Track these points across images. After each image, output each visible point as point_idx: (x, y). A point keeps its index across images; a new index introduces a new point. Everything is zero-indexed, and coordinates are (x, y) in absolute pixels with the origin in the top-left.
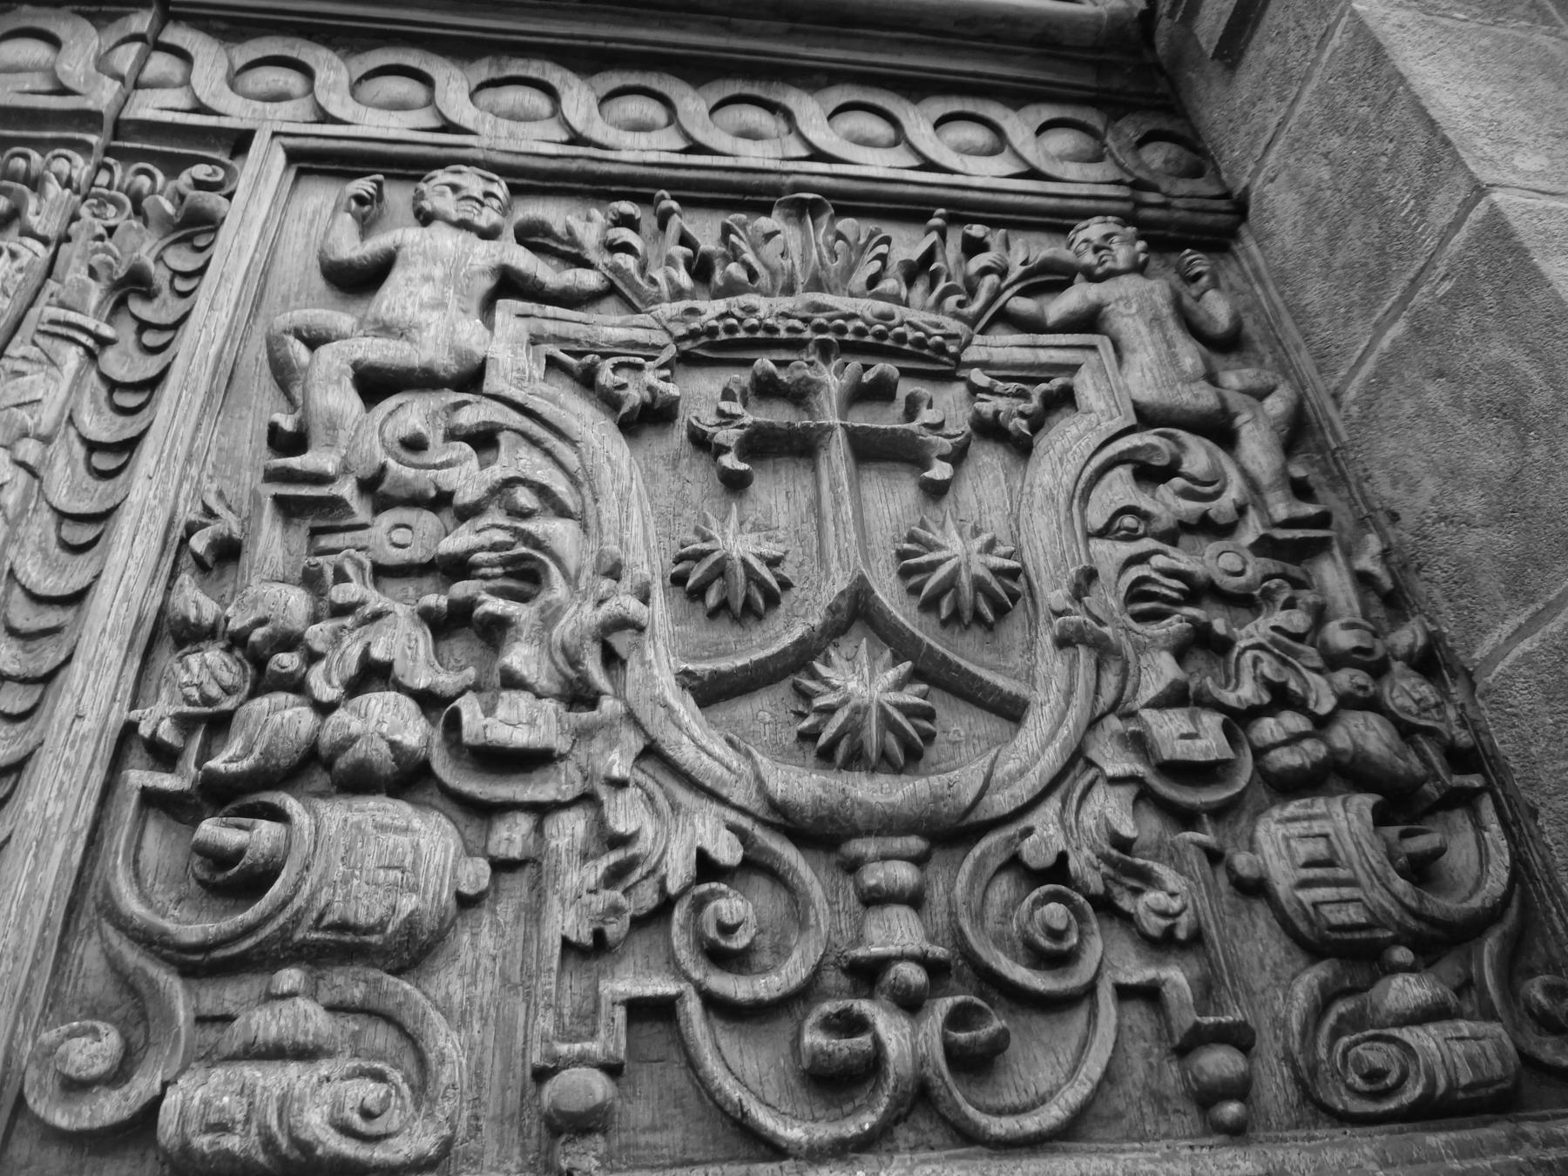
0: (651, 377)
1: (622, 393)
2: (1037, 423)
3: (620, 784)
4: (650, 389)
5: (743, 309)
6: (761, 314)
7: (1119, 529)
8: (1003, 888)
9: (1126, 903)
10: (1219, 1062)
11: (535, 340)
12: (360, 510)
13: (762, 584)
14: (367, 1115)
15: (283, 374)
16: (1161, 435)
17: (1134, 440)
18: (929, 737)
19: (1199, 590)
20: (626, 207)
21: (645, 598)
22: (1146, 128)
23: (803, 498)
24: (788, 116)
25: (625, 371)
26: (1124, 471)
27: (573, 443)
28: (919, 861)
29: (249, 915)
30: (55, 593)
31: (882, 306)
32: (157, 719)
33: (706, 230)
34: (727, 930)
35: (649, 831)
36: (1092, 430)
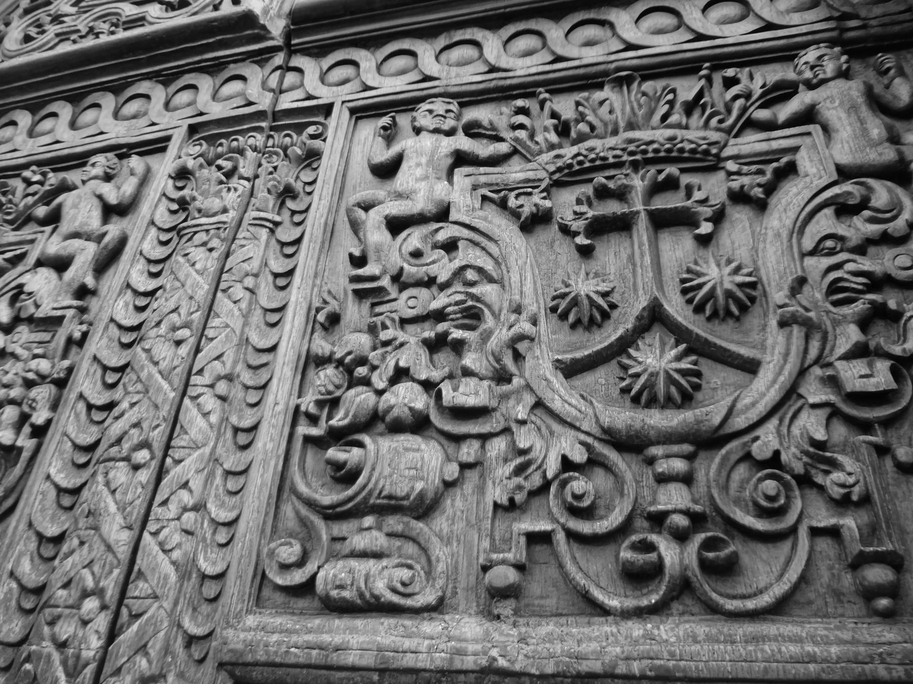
0: (536, 198)
1: (521, 210)
2: (770, 189)
3: (523, 423)
4: (536, 205)
5: (587, 150)
6: (597, 151)
7: (823, 249)
8: (742, 471)
9: (819, 479)
10: (877, 574)
11: (475, 187)
12: (393, 293)
13: (599, 308)
14: (404, 584)
15: (355, 226)
16: (856, 183)
17: (836, 190)
18: (697, 387)
19: (877, 282)
20: (520, 103)
21: (535, 322)
23: (624, 256)
24: (612, 26)
25: (523, 197)
26: (829, 211)
27: (496, 242)
28: (690, 457)
29: (350, 492)
30: (266, 347)
31: (669, 132)
32: (308, 403)
33: (565, 106)
34: (578, 497)
35: (539, 445)
36: (807, 187)
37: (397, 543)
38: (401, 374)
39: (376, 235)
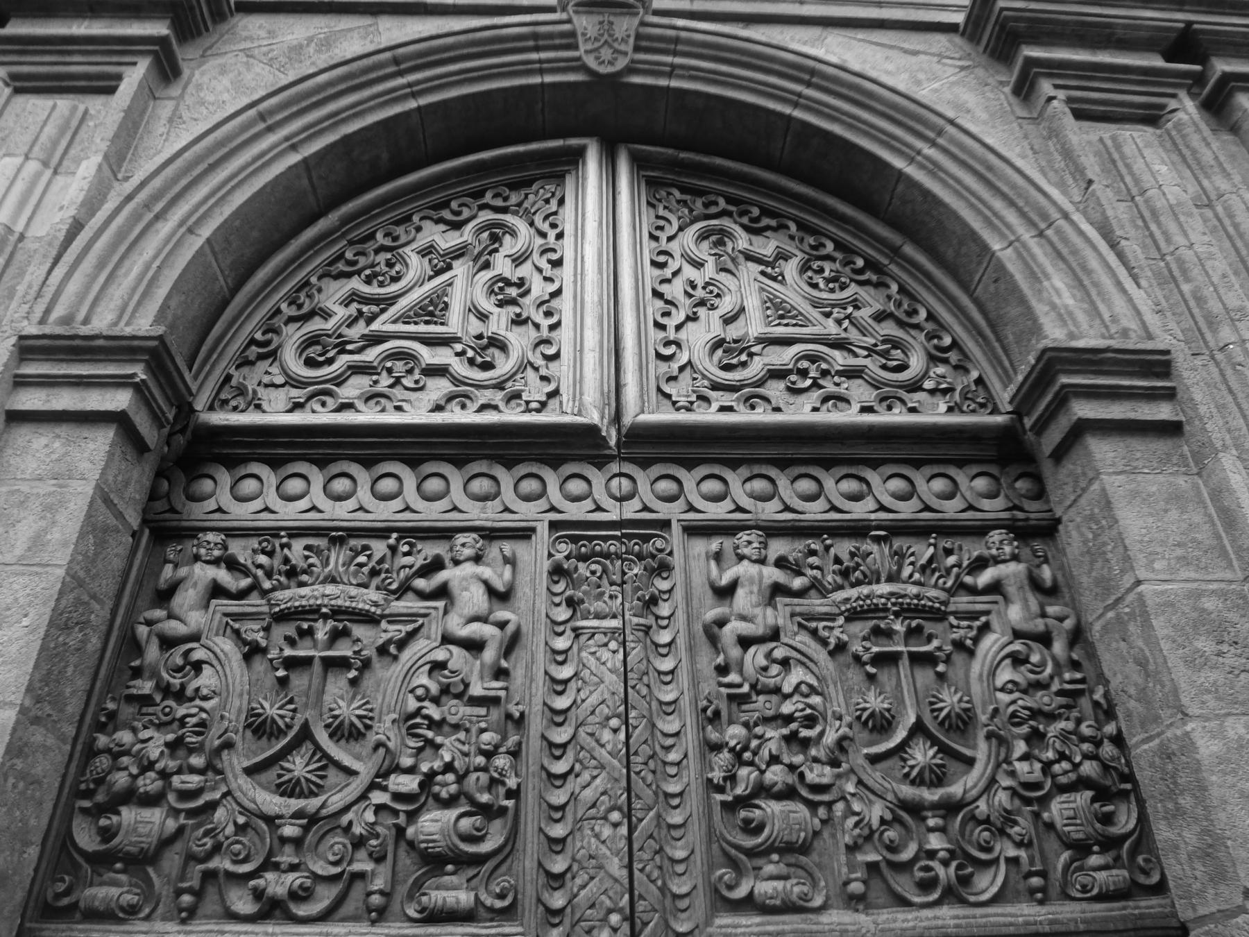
2: (976, 640)
9: (1009, 831)
10: (1036, 881)
11: (793, 615)
13: (887, 719)
19: (1035, 713)
22: (1019, 471)
26: (1008, 661)
28: (943, 817)
32: (717, 775)
34: (891, 841)
37: (792, 870)
38: (774, 759)
39: (735, 652)
